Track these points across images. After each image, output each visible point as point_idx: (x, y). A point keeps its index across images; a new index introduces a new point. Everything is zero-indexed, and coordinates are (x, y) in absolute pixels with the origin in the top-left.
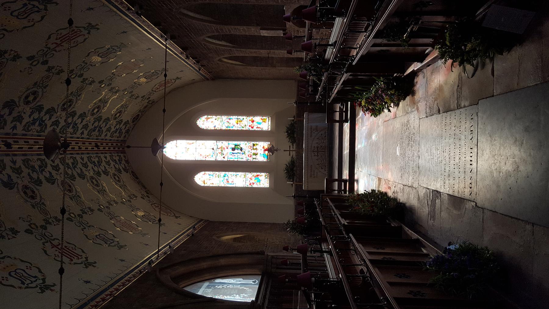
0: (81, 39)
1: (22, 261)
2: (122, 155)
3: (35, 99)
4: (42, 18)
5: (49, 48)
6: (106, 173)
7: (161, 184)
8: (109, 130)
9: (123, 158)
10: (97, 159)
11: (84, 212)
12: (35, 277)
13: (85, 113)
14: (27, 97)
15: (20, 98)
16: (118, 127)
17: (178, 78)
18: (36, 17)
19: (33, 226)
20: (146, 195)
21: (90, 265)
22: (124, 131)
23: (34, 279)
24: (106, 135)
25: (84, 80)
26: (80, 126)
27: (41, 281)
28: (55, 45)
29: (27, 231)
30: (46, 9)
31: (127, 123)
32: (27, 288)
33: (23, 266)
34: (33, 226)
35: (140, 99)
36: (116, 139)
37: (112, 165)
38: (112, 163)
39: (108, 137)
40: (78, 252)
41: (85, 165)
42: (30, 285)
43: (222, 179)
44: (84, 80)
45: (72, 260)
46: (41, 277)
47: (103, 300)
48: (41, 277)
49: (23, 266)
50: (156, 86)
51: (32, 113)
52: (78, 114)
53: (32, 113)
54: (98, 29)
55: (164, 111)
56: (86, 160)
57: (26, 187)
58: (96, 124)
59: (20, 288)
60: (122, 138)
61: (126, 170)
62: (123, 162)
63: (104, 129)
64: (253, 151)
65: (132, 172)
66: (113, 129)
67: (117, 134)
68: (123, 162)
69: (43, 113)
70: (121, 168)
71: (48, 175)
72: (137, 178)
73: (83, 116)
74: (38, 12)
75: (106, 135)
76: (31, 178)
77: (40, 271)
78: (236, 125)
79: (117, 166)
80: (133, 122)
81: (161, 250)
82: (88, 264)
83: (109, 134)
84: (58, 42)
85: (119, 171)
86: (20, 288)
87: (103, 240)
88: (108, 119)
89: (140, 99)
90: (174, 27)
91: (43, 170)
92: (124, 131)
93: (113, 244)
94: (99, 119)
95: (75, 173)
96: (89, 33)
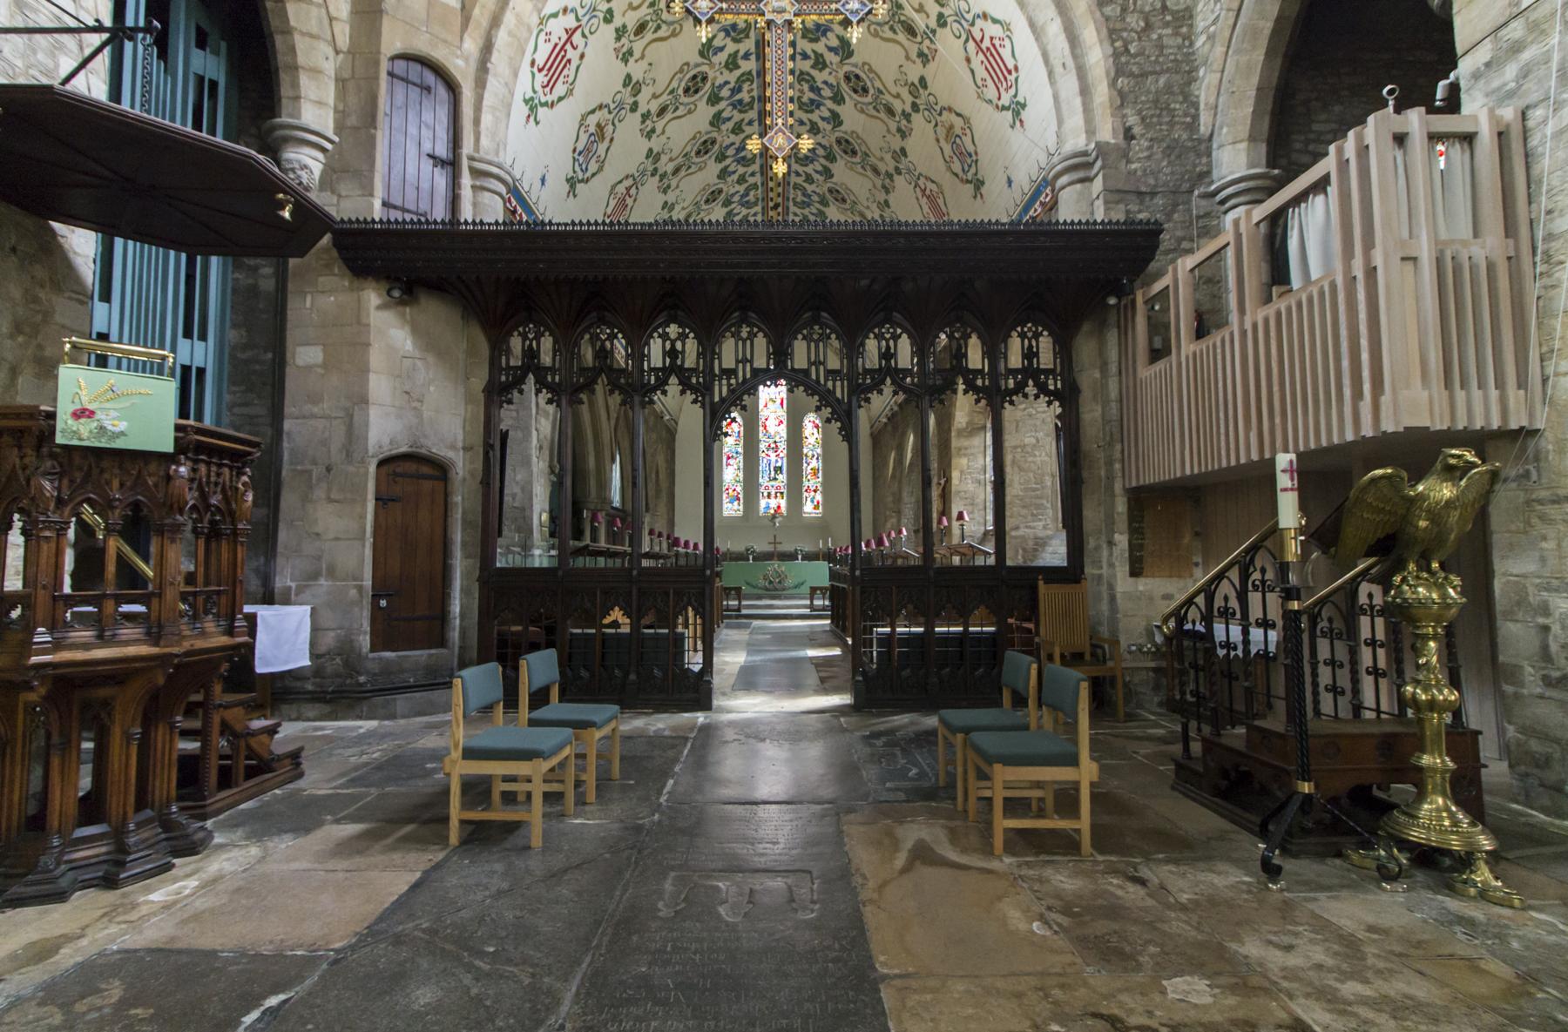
5: (973, 24)
13: (841, 123)
16: (815, 198)
21: (531, 109)
24: (798, 174)
28: (978, 38)
63: (809, 169)
66: (810, 188)
75: (798, 174)
83: (799, 180)
84: (986, 43)
96: (1004, 108)
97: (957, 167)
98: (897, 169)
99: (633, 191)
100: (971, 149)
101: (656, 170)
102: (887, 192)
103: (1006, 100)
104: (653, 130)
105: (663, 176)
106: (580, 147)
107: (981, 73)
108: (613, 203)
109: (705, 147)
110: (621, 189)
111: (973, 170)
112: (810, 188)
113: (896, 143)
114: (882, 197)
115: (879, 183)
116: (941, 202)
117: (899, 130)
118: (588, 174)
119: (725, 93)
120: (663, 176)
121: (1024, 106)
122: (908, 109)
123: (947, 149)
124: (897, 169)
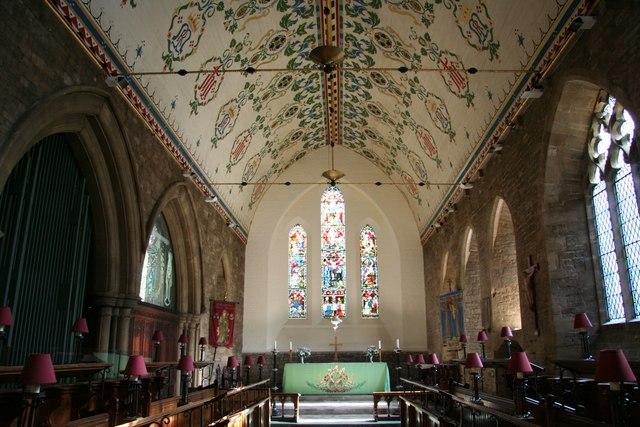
0: (454, 88)
1: (200, 36)
3: (383, 44)
4: (474, 46)
6: (302, 124)
7: (288, 184)
8: (353, 125)
10: (318, 113)
11: (255, 101)
12: (181, 50)
14: (383, 36)
15: (382, 29)
17: (420, 200)
18: (474, 39)
19: (240, 47)
20: (278, 169)
22: (353, 142)
23: (178, 49)
25: (409, 96)
26: (355, 94)
27: (176, 56)
29: (234, 41)
30: (484, 48)
31: (363, 145)
32: (169, 41)
33: (194, 37)
34: (240, 47)
35: (392, 158)
38: (314, 131)
39: (344, 125)
40: (210, 95)
41: (310, 101)
42: (172, 46)
43: (298, 258)
44: (409, 96)
45: (200, 88)
46: (180, 56)
47: (151, 122)
48: (180, 56)
49: (194, 37)
51: (366, 42)
52: (369, 91)
53: (366, 42)
54: (468, 106)
55: (379, 184)
56: (317, 101)
57: (283, 39)
58: (359, 111)
59: (170, 35)
60: (344, 140)
61: (306, 146)
62: (316, 143)
63: (353, 120)
66: (354, 130)
67: (349, 135)
68: (316, 143)
69: (367, 53)
71: (297, 61)
73: (367, 96)
74: (480, 40)
76: (294, 44)
77: (187, 55)
79: (311, 136)
80: (365, 152)
82: (194, 106)
83: (347, 125)
84: (449, 65)
85: (306, 138)
86: (170, 35)
87: (224, 122)
88: (365, 123)
91: (303, 56)
92: (353, 142)
94: (365, 114)
95: (300, 90)
97: (439, 124)
99: (248, 138)
102: (399, 133)
103: (463, 93)
104: (260, 107)
107: (448, 78)
109: (291, 112)
110: (242, 138)
112: (354, 130)
113: (404, 109)
114: (397, 136)
115: (401, 100)
117: (404, 102)
119: (302, 84)
121: (473, 96)
122: (409, 91)
123: (433, 115)
124: (404, 122)
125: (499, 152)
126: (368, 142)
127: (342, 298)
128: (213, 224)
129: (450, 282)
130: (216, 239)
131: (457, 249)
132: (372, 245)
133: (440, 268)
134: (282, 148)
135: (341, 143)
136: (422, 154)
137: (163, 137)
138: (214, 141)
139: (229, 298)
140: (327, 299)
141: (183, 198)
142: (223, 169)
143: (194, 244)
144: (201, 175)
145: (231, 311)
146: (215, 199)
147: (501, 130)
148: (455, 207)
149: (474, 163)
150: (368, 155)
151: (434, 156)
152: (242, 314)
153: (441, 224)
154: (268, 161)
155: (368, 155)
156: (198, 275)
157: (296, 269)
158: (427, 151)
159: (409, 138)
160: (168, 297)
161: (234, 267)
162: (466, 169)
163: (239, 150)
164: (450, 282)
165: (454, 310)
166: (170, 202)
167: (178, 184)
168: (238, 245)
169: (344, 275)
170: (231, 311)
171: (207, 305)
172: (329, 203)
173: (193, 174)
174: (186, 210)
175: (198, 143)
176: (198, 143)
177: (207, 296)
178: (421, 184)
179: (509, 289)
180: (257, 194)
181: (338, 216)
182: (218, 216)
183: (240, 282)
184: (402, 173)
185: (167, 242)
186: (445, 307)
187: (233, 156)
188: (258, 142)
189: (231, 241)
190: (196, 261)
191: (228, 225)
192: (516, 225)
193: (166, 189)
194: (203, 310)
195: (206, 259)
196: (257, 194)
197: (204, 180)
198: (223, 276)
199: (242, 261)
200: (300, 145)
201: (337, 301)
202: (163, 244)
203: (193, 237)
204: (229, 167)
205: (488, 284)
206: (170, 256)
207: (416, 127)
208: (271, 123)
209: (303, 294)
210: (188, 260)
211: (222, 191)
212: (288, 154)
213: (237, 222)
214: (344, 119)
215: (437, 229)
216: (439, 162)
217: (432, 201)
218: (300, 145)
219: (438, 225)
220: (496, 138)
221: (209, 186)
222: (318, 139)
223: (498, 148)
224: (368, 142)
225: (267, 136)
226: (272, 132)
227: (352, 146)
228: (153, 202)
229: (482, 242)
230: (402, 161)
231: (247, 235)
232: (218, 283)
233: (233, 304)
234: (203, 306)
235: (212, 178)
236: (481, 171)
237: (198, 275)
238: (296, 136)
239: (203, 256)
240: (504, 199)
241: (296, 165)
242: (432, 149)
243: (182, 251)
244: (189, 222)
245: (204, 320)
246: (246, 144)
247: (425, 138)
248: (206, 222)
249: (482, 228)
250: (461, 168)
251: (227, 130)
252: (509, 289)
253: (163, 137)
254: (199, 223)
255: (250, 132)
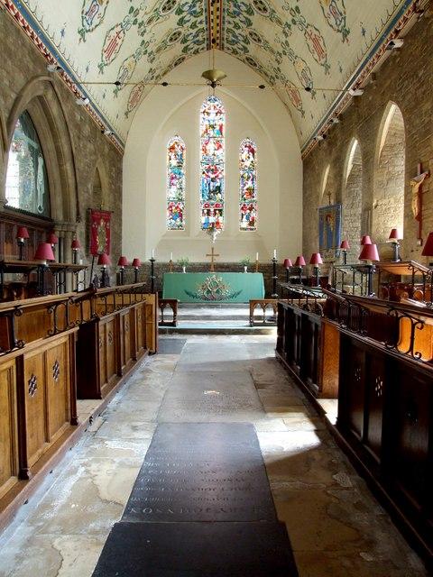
2: (205, 45)
6: (181, 22)
9: (201, 47)
20: (155, 75)
24: (229, 23)
31: (245, 50)
36: (225, 37)
37: (191, 31)
38: (194, 31)
39: (227, 26)
50: (292, 86)
58: (243, 8)
60: (226, 45)
61: (185, 50)
62: (196, 47)
63: (237, 20)
64: (212, 210)
65: (183, 59)
67: (231, 38)
68: (196, 47)
70: (188, 43)
72: (176, 65)
75: (229, 23)
78: (245, 188)
79: (190, 38)
80: (247, 59)
81: (81, 88)
83: (231, 26)
85: (184, 41)
88: (249, 24)
89: (276, 65)
90: (370, 98)
92: (235, 47)
93: (85, 23)
97: (332, 21)
98: (293, 20)
99: (121, 35)
100: (341, 10)
101: (136, 20)
102: (286, 35)
105: (140, 25)
106: (86, 9)
108: (108, 43)
110: (113, 34)
111: (343, 23)
112: (237, 32)
114: (283, 39)
116: (321, 43)
118: (93, 26)
120: (140, 25)
124: (293, 20)
125: (398, 49)
126: (252, 47)
127: (220, 211)
128: (87, 130)
129: (329, 194)
130: (90, 147)
131: (339, 163)
132: (252, 159)
133: (319, 182)
134: (159, 50)
135: (222, 48)
136: (311, 61)
137: (17, 16)
138: (82, 33)
139: (106, 208)
140: (206, 211)
141: (50, 96)
142: (94, 69)
143: (66, 149)
144: (69, 72)
145: (107, 220)
146: (87, 101)
147: (406, 20)
148: (341, 117)
149: (367, 65)
150: (251, 62)
151: (323, 61)
152: (120, 225)
153: (324, 136)
154: (144, 65)
155: (251, 62)
156: (71, 181)
157: (175, 181)
158: (316, 56)
159: (298, 41)
160: (40, 203)
161: (111, 177)
162: (358, 73)
163: (111, 48)
164: (329, 194)
165: (332, 223)
166: (33, 100)
167: (42, 78)
168: (115, 155)
169: (223, 188)
170: (107, 220)
171: (83, 215)
172: (208, 114)
173: (58, 68)
174: (54, 110)
175: (63, 32)
176: (63, 32)
177: (83, 205)
178: (308, 89)
179: (392, 200)
180: (134, 101)
181: (218, 128)
182: (91, 121)
183: (117, 193)
184: (286, 82)
185: (35, 145)
186: (324, 223)
187: (105, 55)
188: (132, 41)
189: (107, 150)
190: (68, 167)
191: (103, 132)
192: (408, 131)
193: (28, 82)
194: (78, 219)
195: (80, 165)
196: (134, 101)
197: (73, 78)
198: (98, 187)
199: (119, 172)
200: (178, 48)
201: (215, 214)
202: (31, 147)
203: (63, 140)
204: (101, 67)
205: (369, 194)
206: (40, 161)
207: (305, 26)
208: (146, 19)
209: (181, 207)
210: (60, 166)
211: (94, 92)
212: (165, 58)
213: (112, 130)
214: (227, 18)
215: (320, 142)
216: (327, 67)
217: (316, 113)
218: (178, 48)
219: (320, 138)
220: (397, 32)
221: (78, 84)
222: (198, 43)
223: (398, 44)
224: (252, 47)
225: (142, 34)
226: (148, 29)
227: (235, 52)
228: (14, 96)
229: (367, 155)
230: (288, 68)
231: (124, 146)
232: (95, 193)
233: (109, 213)
234: (78, 214)
235: (82, 76)
236: (374, 76)
237: (71, 181)
238: (174, 37)
239: (76, 161)
240: (398, 103)
241: (175, 70)
242: (321, 53)
243: (52, 156)
244: (59, 125)
245: (80, 230)
246: (119, 41)
247: (315, 41)
248: (78, 127)
249: (369, 137)
250: (351, 73)
251: (96, 21)
252: (392, 200)
253: (17, 16)
254: (70, 126)
255: (123, 27)
